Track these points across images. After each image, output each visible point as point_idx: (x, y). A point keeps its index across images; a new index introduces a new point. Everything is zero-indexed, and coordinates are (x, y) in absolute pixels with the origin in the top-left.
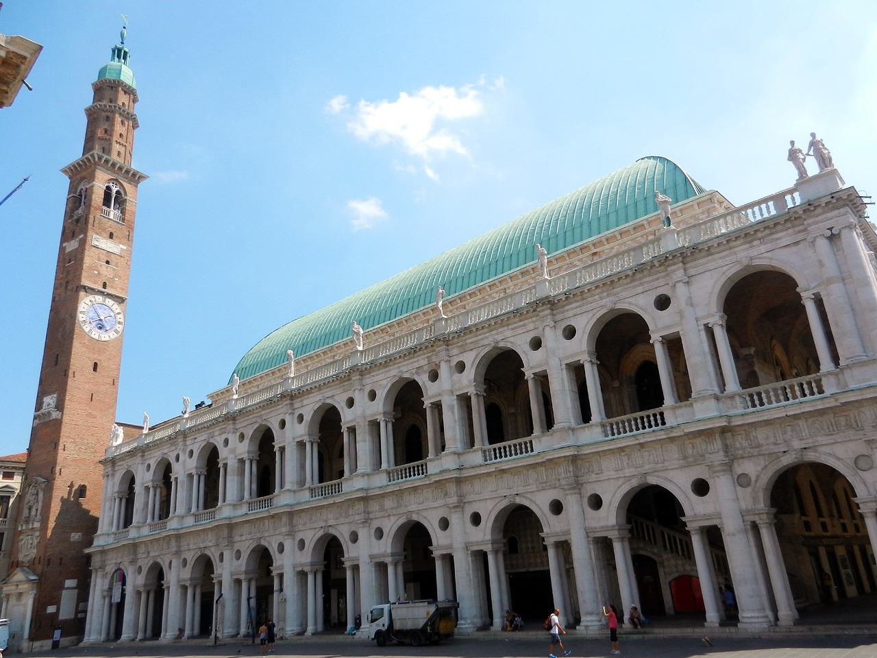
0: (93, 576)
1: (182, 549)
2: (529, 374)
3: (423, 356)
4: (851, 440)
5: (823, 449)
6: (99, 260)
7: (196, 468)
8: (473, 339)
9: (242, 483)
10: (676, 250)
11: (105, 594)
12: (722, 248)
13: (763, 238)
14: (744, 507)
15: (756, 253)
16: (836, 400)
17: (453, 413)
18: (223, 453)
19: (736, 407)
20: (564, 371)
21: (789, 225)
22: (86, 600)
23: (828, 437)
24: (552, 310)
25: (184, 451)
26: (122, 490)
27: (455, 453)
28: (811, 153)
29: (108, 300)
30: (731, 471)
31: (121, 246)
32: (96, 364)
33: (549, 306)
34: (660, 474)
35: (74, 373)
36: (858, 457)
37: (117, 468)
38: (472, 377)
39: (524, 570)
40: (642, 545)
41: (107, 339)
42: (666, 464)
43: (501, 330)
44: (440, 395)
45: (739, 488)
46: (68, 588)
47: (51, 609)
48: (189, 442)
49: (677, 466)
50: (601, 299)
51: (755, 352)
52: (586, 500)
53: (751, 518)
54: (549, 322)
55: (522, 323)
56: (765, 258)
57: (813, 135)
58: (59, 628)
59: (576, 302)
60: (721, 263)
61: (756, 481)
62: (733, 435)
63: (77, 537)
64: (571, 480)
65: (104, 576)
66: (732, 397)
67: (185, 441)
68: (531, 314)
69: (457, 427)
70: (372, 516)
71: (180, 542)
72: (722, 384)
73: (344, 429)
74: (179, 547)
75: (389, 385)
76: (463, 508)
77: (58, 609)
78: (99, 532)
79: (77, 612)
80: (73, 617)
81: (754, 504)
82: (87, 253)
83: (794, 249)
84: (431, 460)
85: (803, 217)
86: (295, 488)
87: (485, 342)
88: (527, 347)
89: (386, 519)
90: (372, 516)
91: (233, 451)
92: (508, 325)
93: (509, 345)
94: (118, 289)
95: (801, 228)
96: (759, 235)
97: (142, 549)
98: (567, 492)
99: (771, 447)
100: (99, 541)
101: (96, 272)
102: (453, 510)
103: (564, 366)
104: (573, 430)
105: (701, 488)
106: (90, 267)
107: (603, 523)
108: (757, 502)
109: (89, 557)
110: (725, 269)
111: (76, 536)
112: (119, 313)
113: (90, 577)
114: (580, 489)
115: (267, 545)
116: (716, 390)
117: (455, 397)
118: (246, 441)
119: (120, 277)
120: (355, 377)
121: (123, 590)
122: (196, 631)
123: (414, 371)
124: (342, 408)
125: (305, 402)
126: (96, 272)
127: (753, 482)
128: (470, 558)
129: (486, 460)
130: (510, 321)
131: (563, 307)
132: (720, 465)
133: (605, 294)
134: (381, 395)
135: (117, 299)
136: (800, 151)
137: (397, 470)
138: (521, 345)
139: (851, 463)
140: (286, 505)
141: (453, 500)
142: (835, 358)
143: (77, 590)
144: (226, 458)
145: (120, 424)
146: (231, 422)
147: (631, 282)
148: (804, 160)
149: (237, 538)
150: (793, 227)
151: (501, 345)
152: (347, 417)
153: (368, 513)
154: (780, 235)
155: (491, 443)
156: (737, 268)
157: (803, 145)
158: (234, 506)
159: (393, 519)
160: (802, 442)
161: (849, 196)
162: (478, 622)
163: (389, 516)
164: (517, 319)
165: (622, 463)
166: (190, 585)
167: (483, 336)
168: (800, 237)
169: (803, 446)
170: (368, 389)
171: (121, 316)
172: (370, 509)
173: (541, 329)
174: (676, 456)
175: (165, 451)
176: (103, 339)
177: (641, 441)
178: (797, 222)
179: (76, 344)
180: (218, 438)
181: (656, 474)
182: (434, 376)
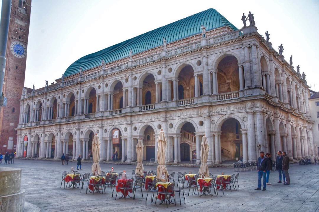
0: (18, 137)
1: (45, 131)
2: (156, 83)
3: (124, 74)
4: (243, 112)
5: (236, 114)
7: (50, 105)
8: (140, 69)
9: (64, 111)
10: (204, 46)
11: (22, 143)
12: (218, 47)
13: (231, 45)
14: (212, 130)
15: (228, 50)
16: (240, 100)
17: (132, 94)
18: (59, 101)
19: (215, 99)
20: (167, 83)
21: (238, 42)
22: (16, 144)
23: (238, 111)
24: (165, 62)
25: (46, 99)
26: (26, 110)
27: (131, 107)
28: (248, 18)
29: (21, 43)
30: (210, 119)
31: (26, 23)
33: (165, 60)
34: (190, 119)
36: (244, 117)
37: (25, 103)
38: (138, 82)
39: (151, 146)
40: (186, 140)
41: (21, 57)
42: (193, 116)
43: (149, 67)
44: (128, 87)
45: (211, 125)
46: (10, 140)
48: (47, 96)
50: (181, 60)
51: (231, 81)
52: (168, 125)
53: (212, 133)
54: (164, 66)
55: (156, 65)
56: (231, 52)
57: (250, 12)
59: (173, 60)
60: (218, 52)
61: (216, 123)
62: (213, 108)
63: (12, 124)
64: (164, 119)
65: (21, 137)
66: (214, 96)
67: (46, 96)
68: (159, 63)
69: (133, 99)
70: (104, 125)
71: (44, 129)
72: (212, 92)
73: (97, 96)
74: (44, 130)
76: (132, 125)
77: (7, 146)
78: (19, 123)
79: (13, 147)
80: (12, 149)
81: (215, 129)
83: (239, 50)
84: (124, 109)
85: (242, 40)
86: (80, 114)
87: (144, 71)
88: (157, 74)
89: (108, 127)
90: (104, 125)
91: (62, 100)
92: (151, 65)
93: (151, 73)
94: (25, 39)
95: (241, 43)
96: (230, 44)
97: (33, 130)
98: (163, 122)
99: (222, 112)
100: (19, 126)
101: (16, 32)
102: (128, 125)
103: (167, 81)
104: (167, 102)
105: (202, 123)
107: (173, 132)
108: (216, 129)
109: (16, 131)
110: (219, 54)
111: (12, 124)
112: (25, 48)
113: (17, 137)
114: (167, 122)
115: (71, 132)
116: (210, 94)
117: (133, 89)
118: (66, 98)
119: (25, 35)
120: (101, 79)
121: (27, 142)
122: (50, 156)
123: (121, 79)
124: (97, 89)
125: (85, 86)
126: (16, 32)
127: (215, 123)
128: (132, 141)
129: (140, 110)
130: (152, 64)
131: (169, 61)
132: (207, 117)
133: (182, 58)
134: (109, 85)
135: (24, 43)
136: (245, 17)
137: (113, 111)
138: (155, 72)
139: (242, 119)
140: (77, 120)
141: (129, 122)
142: (244, 86)
143: (13, 141)
144: (59, 103)
145: (26, 88)
146: (61, 91)
147: (191, 55)
148: (246, 21)
150: (240, 42)
151: (149, 72)
152: (98, 92)
153: (103, 124)
154: (236, 45)
155: (143, 105)
156: (222, 54)
157: (247, 15)
158: (61, 118)
159: (110, 127)
160: (231, 112)
161: (256, 34)
162: (133, 160)
163: (109, 126)
164: (154, 64)
165: (180, 114)
166: (48, 142)
167: (143, 68)
168: (241, 46)
169: (231, 113)
170: (105, 83)
171: (25, 49)
172: (103, 123)
173: (161, 68)
174: (196, 113)
175: (40, 99)
176: (19, 57)
177: (186, 108)
178: (240, 41)
180: (56, 96)
181: (189, 118)
182: (127, 80)
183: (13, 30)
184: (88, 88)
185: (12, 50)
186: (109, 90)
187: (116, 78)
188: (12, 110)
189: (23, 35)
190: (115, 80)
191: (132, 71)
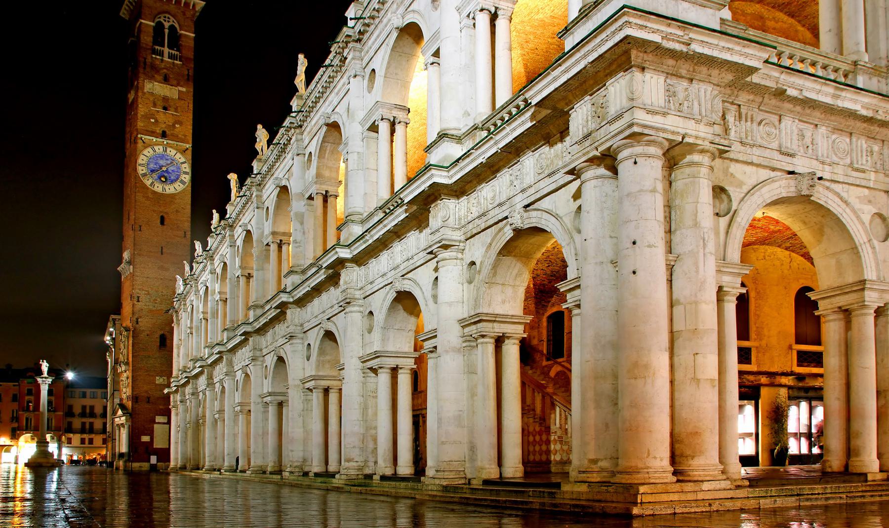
6: (155, 105)
35: (140, 226)
49: (422, 262)
75: (275, 199)
82: (140, 100)
101: (153, 120)
106: (147, 117)
118: (219, 281)
126: (153, 120)
169: (526, 202)
176: (168, 192)
179: (140, 197)
183: (142, 113)
184: (244, 236)
186: (271, 230)
187: (277, 178)
189: (174, 125)
190: (279, 189)
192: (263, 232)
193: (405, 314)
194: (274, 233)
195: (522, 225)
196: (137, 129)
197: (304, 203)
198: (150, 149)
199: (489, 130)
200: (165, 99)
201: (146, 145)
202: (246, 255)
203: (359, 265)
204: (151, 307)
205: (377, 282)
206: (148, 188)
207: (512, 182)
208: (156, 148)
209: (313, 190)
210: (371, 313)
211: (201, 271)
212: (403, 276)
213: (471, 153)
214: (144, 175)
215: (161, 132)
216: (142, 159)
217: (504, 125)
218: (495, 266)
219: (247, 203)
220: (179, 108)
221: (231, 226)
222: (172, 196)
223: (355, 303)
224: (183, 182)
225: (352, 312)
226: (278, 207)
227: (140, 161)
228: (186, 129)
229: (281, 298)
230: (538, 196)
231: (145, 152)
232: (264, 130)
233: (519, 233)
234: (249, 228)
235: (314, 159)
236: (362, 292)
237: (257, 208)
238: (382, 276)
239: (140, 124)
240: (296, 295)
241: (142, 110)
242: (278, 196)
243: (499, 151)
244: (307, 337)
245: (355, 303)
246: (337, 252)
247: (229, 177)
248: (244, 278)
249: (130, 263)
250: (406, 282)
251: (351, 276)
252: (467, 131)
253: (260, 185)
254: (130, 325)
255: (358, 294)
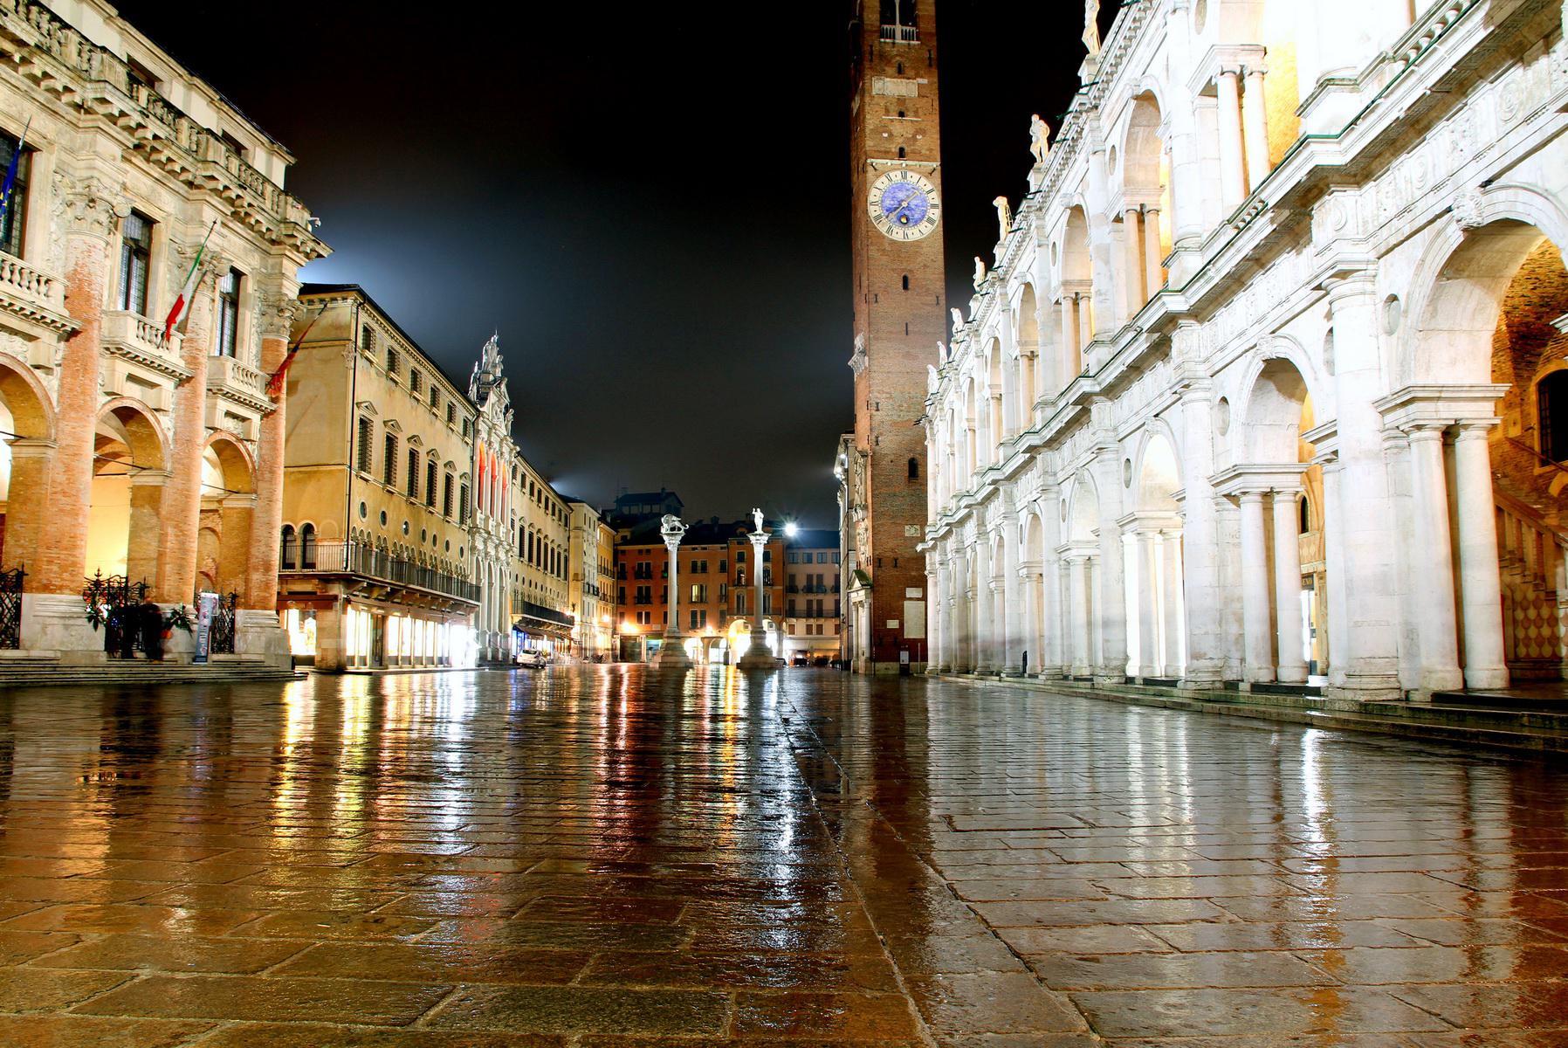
6: (887, 112)
31: (921, 81)
32: (905, 280)
46: (911, 599)
47: (893, 624)
58: (905, 649)
77: (902, 624)
82: (867, 108)
101: (885, 135)
106: (877, 131)
126: (885, 135)
149: (989, 527)
176: (912, 238)
179: (873, 252)
183: (872, 127)
185: (877, 214)
187: (1065, 195)
188: (907, 468)
189: (914, 136)
190: (1069, 211)
191: (1099, 118)
192: (1049, 284)
193: (1281, 398)
194: (1066, 283)
195: (1479, 219)
196: (865, 153)
197: (1108, 230)
198: (883, 179)
199: (1407, 60)
200: (901, 100)
201: (879, 173)
202: (1026, 322)
203: (1201, 321)
204: (895, 418)
205: (1231, 347)
206: (884, 237)
207: (1455, 145)
208: (892, 175)
209: (1121, 207)
210: (1224, 400)
211: (963, 355)
212: (1273, 332)
213: (1378, 105)
214: (878, 218)
215: (898, 150)
216: (874, 195)
217: (1435, 45)
218: (1434, 300)
219: (1023, 241)
220: (920, 110)
221: (1002, 280)
222: (918, 244)
223: (1197, 386)
224: (931, 221)
225: (1190, 401)
226: (1069, 240)
227: (871, 198)
228: (931, 140)
229: (1082, 386)
230: (1507, 161)
231: (878, 184)
232: (1042, 123)
233: (1475, 235)
234: (1029, 279)
235: (1121, 156)
236: (1207, 365)
237: (1039, 246)
238: (1240, 335)
239: (869, 144)
240: (1104, 380)
241: (871, 121)
242: (1069, 223)
243: (1429, 92)
244: (1124, 447)
245: (1197, 386)
246: (1164, 304)
247: (995, 203)
248: (1026, 360)
249: (864, 353)
250: (1279, 342)
251: (1186, 339)
252: (1368, 68)
253: (1040, 209)
254: (867, 447)
255: (1202, 370)
